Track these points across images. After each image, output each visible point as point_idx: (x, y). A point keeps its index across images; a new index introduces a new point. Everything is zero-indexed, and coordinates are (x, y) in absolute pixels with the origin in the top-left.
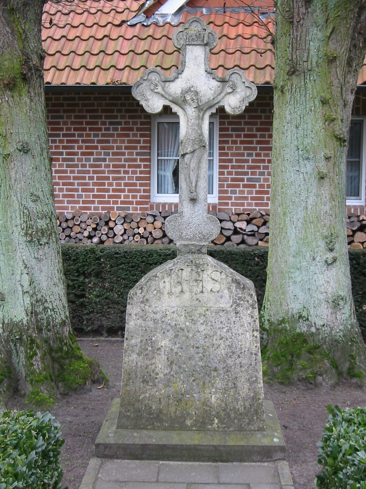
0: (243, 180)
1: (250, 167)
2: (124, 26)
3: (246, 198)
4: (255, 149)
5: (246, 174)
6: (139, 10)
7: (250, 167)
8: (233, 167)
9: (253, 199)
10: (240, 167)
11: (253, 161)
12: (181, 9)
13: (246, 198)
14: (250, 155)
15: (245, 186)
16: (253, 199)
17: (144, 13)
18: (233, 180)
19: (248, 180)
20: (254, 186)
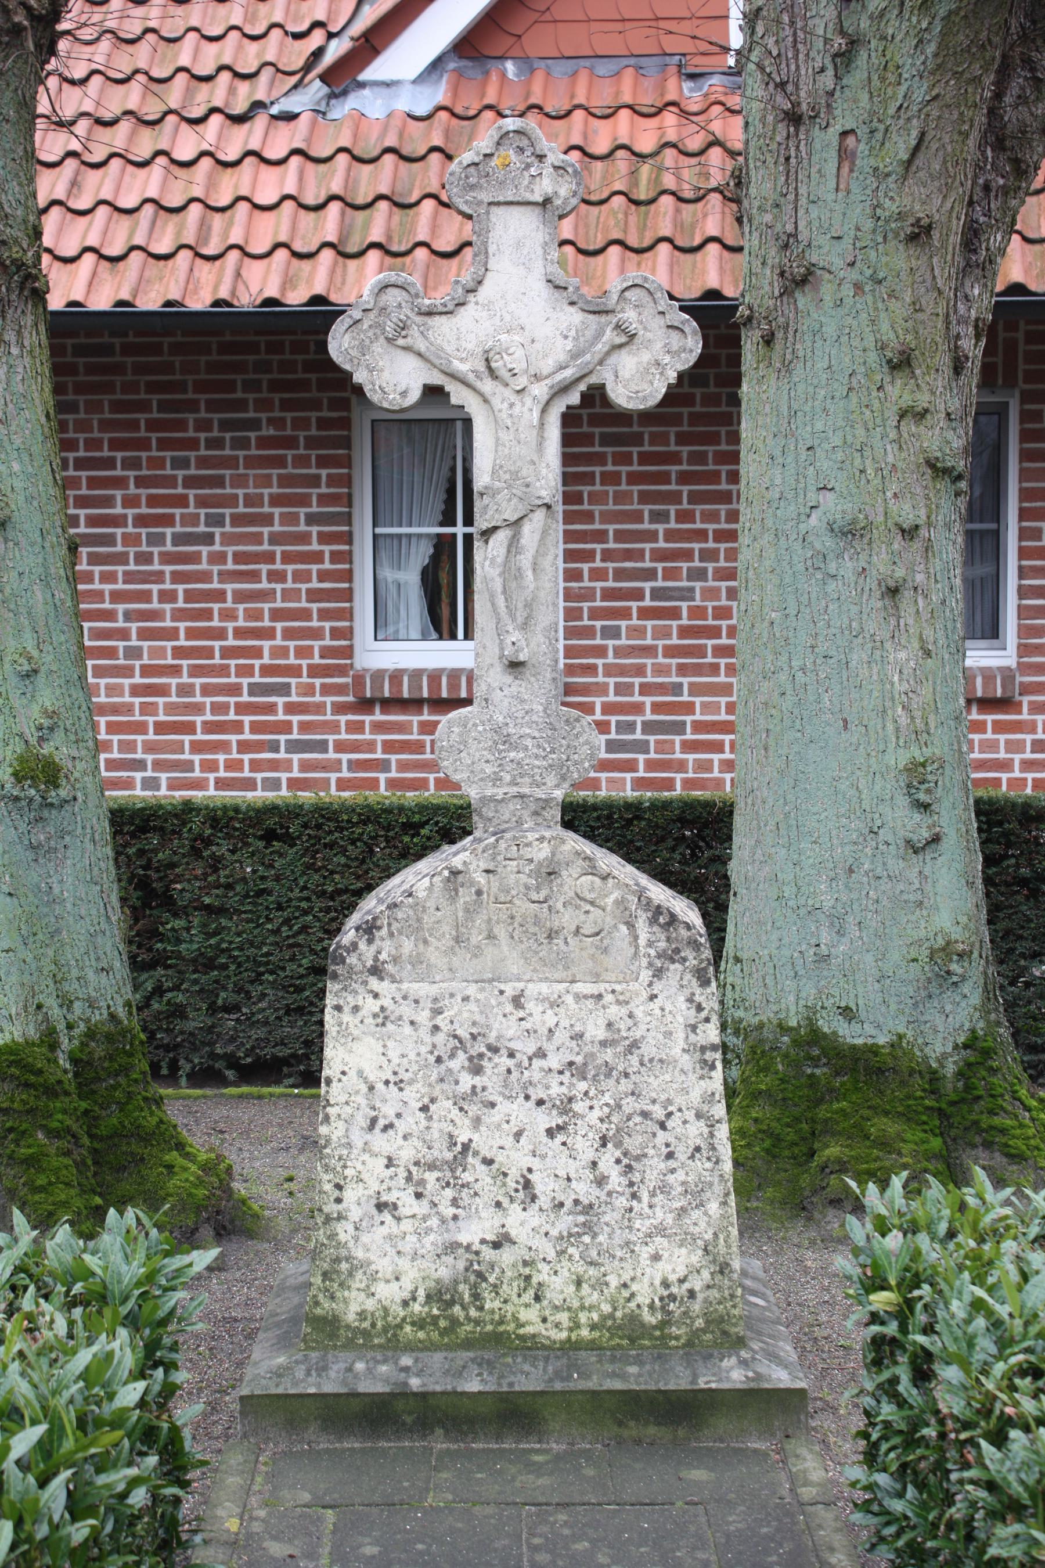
0: (638, 595)
1: (660, 556)
2: (261, 121)
3: (649, 651)
4: (674, 498)
5: (650, 575)
6: (307, 68)
7: (660, 556)
8: (607, 556)
9: (671, 652)
10: (628, 555)
11: (670, 536)
12: (436, 65)
13: (649, 651)
14: (659, 517)
15: (645, 613)
16: (671, 652)
17: (324, 78)
18: (609, 594)
19: (656, 594)
20: (674, 614)
